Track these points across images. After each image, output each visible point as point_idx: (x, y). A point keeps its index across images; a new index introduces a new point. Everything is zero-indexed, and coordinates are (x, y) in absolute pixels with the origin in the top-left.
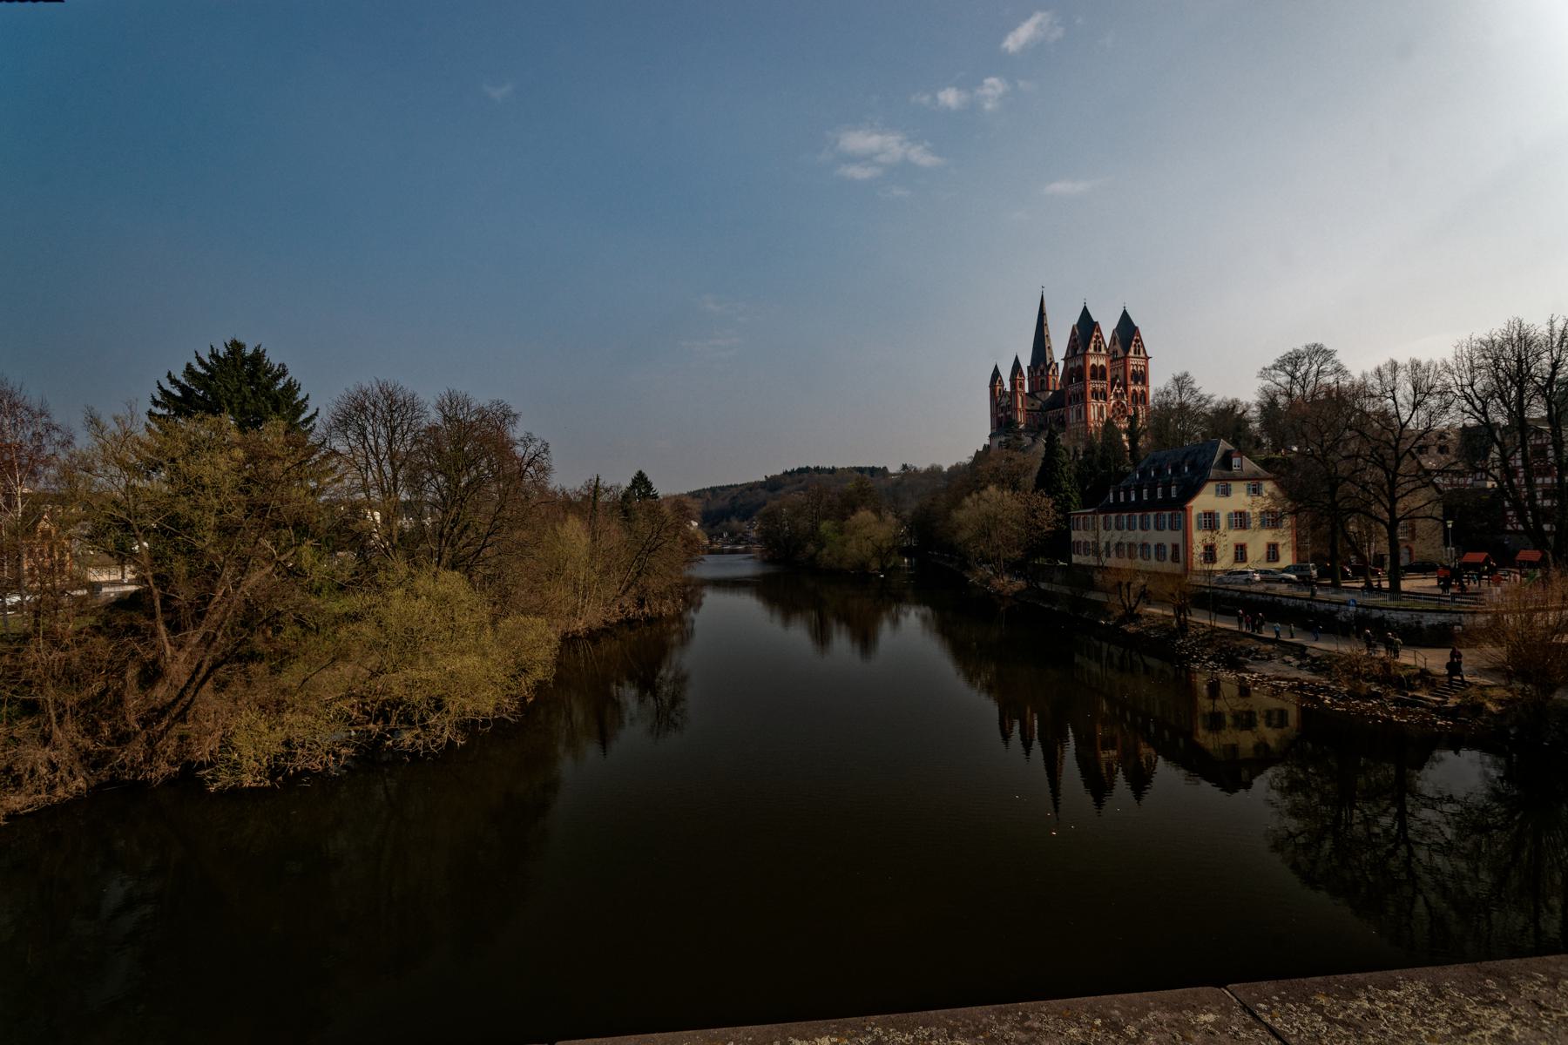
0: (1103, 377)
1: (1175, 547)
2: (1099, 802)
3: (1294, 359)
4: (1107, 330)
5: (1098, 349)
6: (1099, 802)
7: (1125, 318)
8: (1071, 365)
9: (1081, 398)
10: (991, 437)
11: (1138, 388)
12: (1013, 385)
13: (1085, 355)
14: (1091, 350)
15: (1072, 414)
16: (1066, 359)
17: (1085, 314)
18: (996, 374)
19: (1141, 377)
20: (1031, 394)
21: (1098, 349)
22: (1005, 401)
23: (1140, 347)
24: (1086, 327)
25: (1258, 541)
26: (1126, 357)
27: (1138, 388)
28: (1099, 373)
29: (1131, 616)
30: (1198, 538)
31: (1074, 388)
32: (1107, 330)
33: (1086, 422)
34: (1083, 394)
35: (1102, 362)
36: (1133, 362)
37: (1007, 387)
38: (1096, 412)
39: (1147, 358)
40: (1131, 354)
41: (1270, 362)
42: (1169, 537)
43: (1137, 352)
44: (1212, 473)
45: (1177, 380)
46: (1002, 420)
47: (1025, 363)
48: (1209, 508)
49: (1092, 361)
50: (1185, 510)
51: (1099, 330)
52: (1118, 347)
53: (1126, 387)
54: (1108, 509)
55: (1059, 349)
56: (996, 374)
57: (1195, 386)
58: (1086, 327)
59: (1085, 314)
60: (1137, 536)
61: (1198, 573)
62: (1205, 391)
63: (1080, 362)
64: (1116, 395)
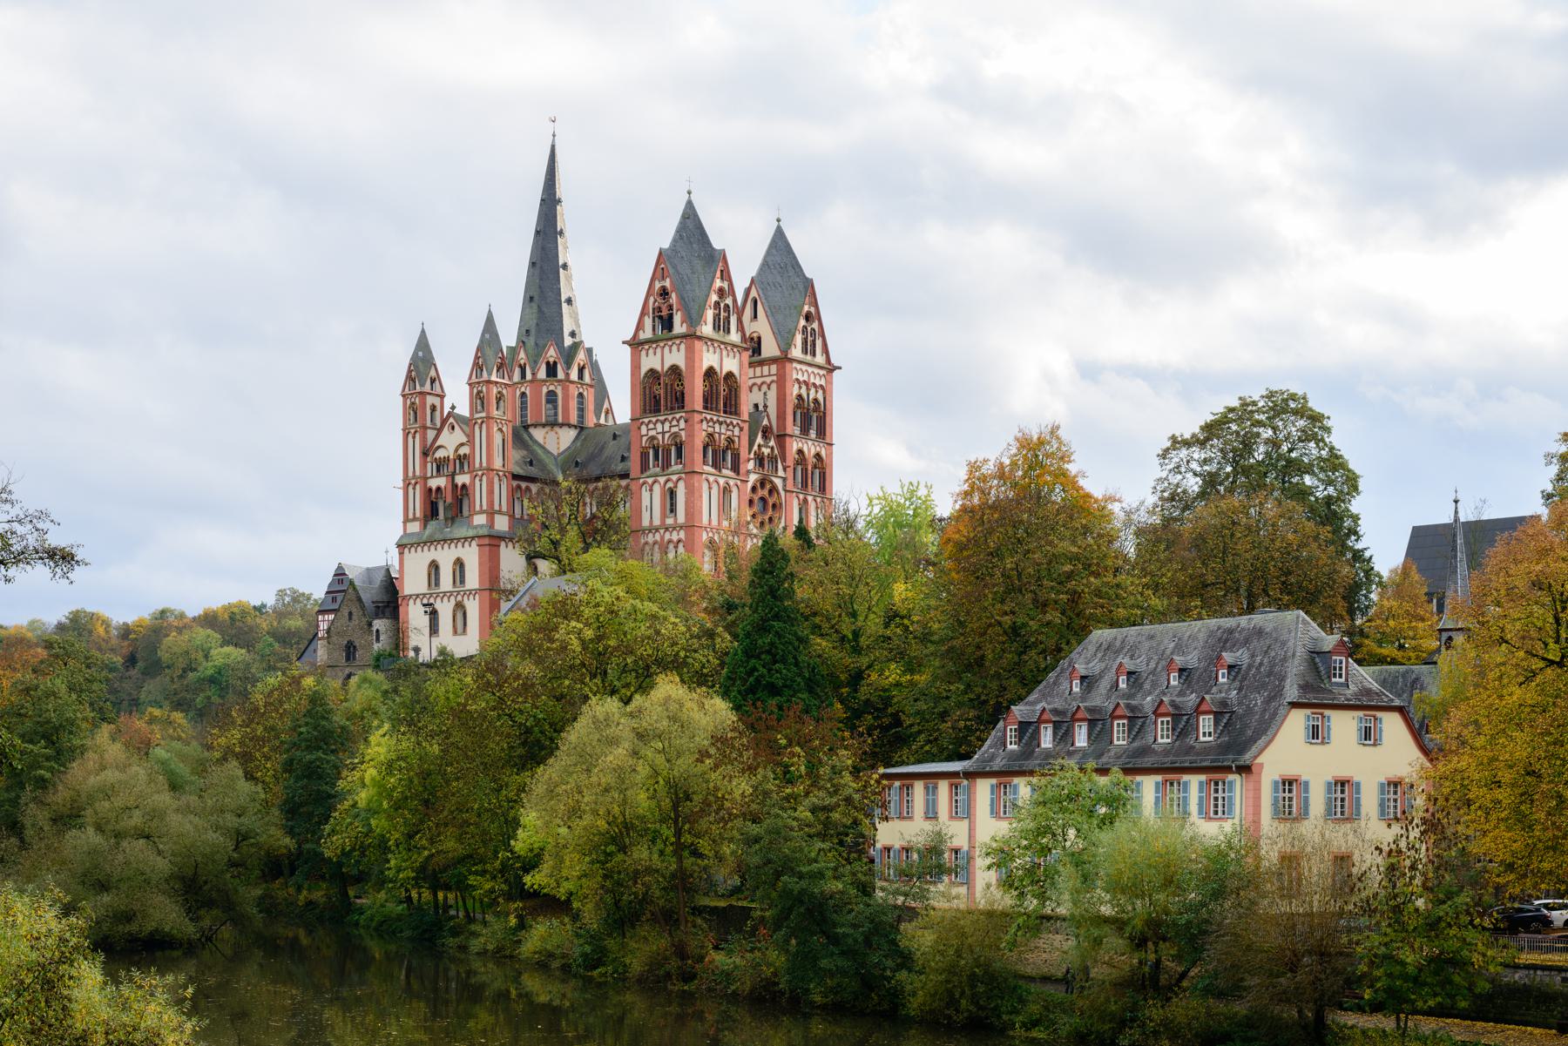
0: (731, 407)
7: (780, 252)
8: (651, 361)
10: (401, 546)
11: (810, 448)
12: (478, 399)
14: (707, 329)
16: (636, 344)
19: (814, 417)
21: (721, 325)
22: (450, 442)
23: (814, 339)
26: (783, 360)
27: (810, 448)
31: (660, 429)
33: (690, 527)
36: (797, 373)
37: (457, 397)
39: (830, 368)
40: (796, 352)
41: (1190, 427)
43: (808, 348)
47: (508, 337)
48: (1291, 772)
49: (709, 359)
51: (726, 275)
53: (782, 438)
55: (606, 313)
56: (422, 370)
57: (1072, 468)
59: (691, 228)
62: (1094, 486)
63: (675, 356)
64: (760, 460)
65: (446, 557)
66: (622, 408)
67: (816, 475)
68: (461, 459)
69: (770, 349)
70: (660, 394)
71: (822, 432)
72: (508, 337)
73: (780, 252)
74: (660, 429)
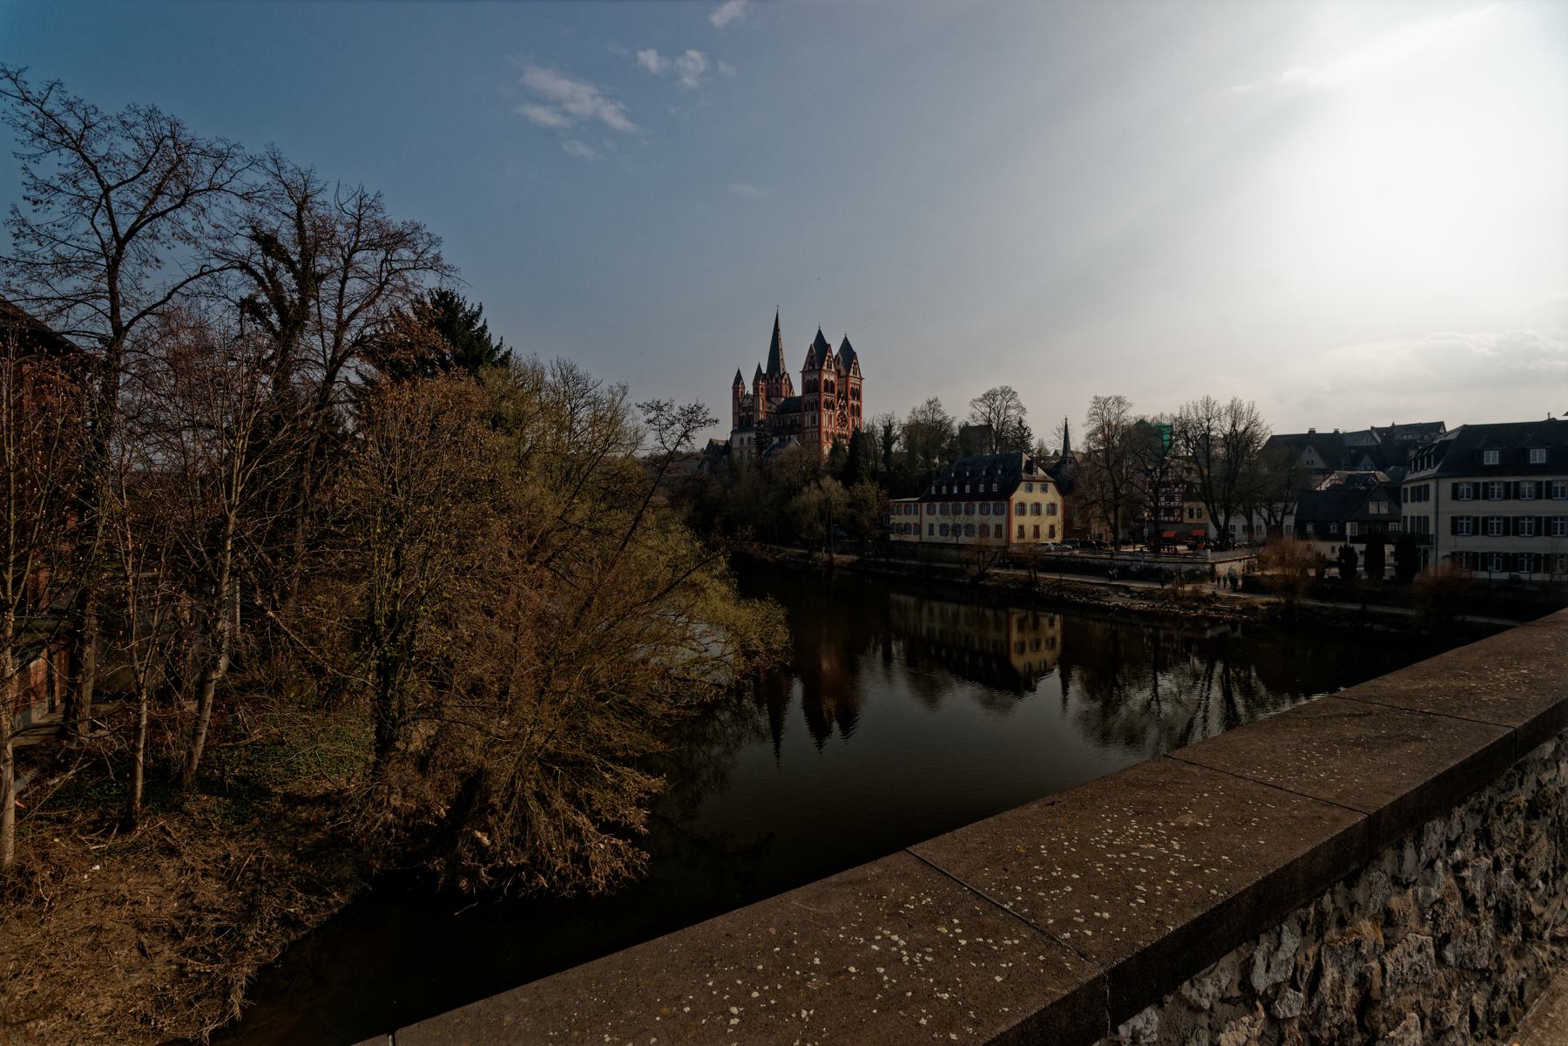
1: (999, 527)
2: (820, 745)
3: (990, 396)
4: (835, 350)
5: (829, 366)
6: (820, 745)
7: (846, 346)
9: (816, 407)
11: (855, 403)
12: (756, 389)
13: (820, 370)
15: (808, 421)
17: (820, 336)
18: (738, 378)
19: (857, 394)
20: (768, 399)
21: (829, 366)
22: (747, 403)
23: (857, 371)
24: (821, 345)
25: (1045, 522)
26: (847, 376)
27: (855, 403)
28: (830, 387)
29: (982, 575)
30: (1017, 521)
31: (810, 398)
32: (835, 350)
33: (820, 427)
34: (818, 403)
35: (832, 378)
36: (852, 380)
37: (749, 389)
38: (828, 422)
42: (993, 520)
44: (1024, 475)
45: (930, 403)
46: (743, 420)
47: (764, 371)
49: (825, 377)
50: (1008, 500)
52: (841, 367)
54: (931, 499)
56: (738, 378)
58: (821, 345)
59: (820, 336)
60: (962, 519)
61: (1018, 545)
63: (816, 376)
65: (746, 436)
66: (798, 392)
67: (857, 411)
68: (751, 408)
69: (843, 373)
70: (811, 386)
71: (859, 398)
72: (764, 371)
73: (846, 346)
74: (810, 398)
